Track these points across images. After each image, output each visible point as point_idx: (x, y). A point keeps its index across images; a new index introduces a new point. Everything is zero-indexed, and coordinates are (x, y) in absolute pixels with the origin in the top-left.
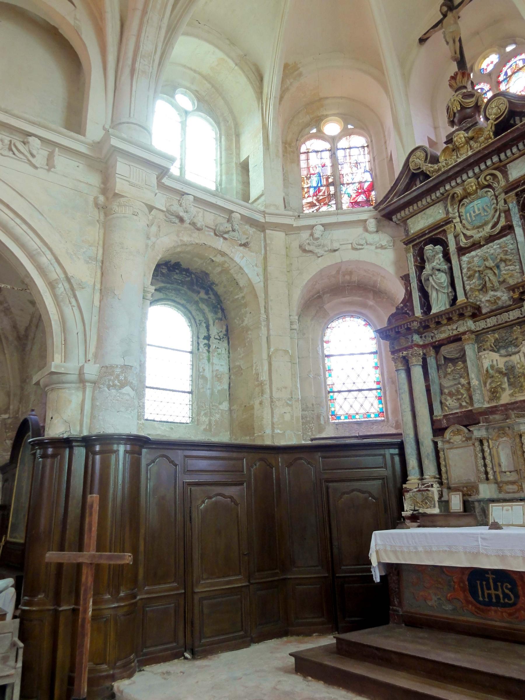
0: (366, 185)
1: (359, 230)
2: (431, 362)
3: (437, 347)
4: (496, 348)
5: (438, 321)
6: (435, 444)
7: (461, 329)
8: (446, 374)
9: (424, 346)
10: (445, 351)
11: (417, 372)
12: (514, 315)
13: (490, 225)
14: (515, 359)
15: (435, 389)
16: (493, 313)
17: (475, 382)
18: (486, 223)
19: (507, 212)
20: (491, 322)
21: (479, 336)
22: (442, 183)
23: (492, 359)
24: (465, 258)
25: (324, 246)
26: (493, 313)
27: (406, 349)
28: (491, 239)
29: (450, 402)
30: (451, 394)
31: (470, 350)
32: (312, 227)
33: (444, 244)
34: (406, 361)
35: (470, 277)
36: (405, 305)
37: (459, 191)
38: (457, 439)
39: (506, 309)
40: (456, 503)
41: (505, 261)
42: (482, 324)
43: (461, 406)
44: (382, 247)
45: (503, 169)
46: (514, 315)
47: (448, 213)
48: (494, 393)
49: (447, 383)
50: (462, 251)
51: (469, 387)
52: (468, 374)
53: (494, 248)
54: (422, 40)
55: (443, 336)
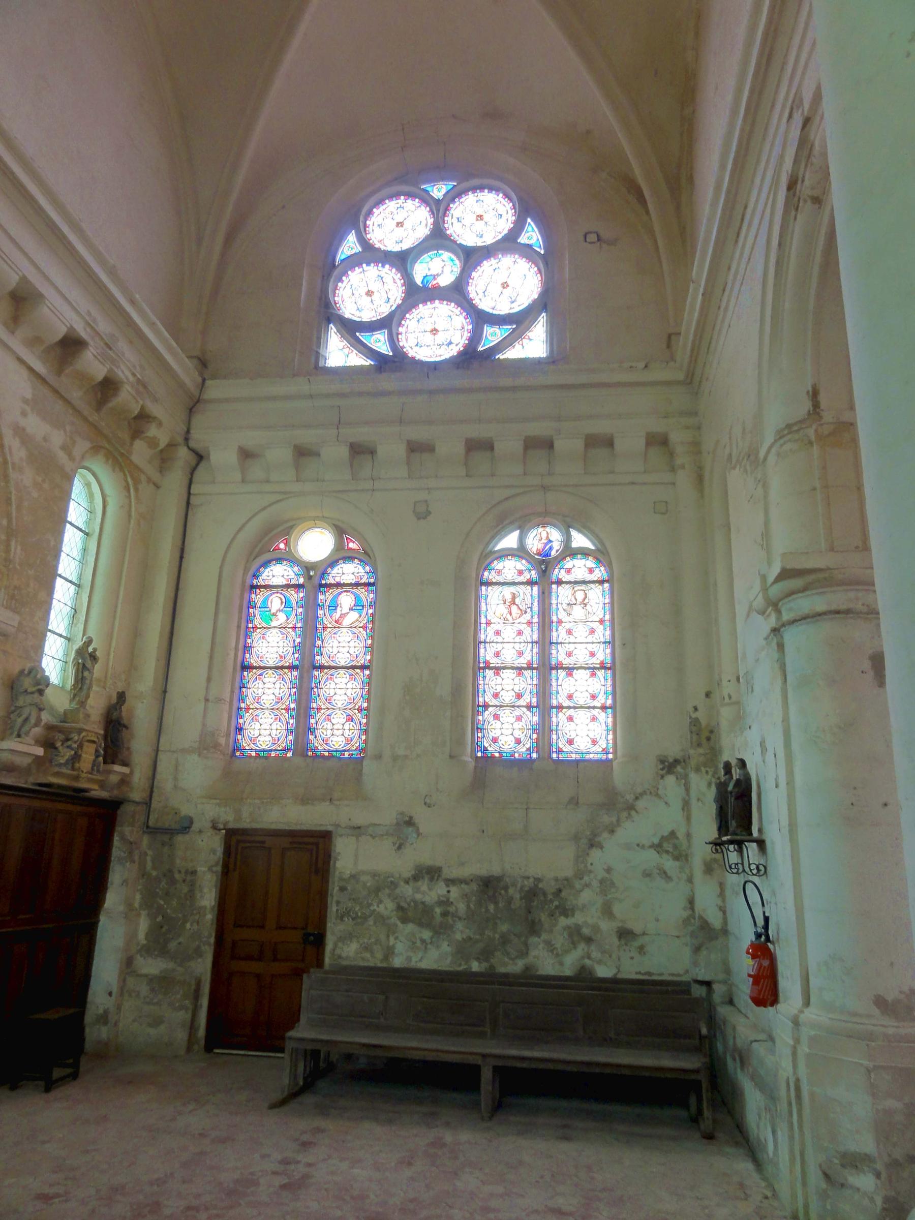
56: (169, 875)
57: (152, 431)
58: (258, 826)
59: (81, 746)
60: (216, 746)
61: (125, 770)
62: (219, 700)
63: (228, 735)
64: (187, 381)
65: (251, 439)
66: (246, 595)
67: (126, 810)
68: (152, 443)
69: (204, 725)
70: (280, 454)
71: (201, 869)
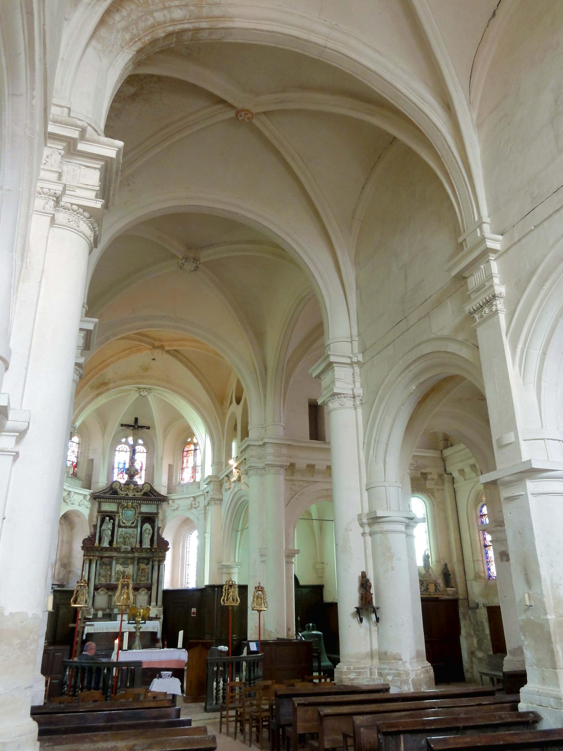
0: (75, 464)
1: (82, 497)
2: (98, 562)
3: (102, 558)
4: (121, 564)
5: (106, 549)
6: (94, 593)
7: (114, 555)
8: (101, 568)
9: (98, 556)
10: (104, 560)
11: (94, 565)
12: (130, 555)
13: (131, 522)
14: (126, 570)
15: (97, 573)
16: (124, 552)
17: (113, 574)
18: (130, 520)
19: (138, 520)
20: (123, 555)
21: (117, 559)
22: (121, 499)
23: (120, 568)
24: (120, 529)
25: (71, 501)
26: (124, 552)
27: (93, 556)
28: (130, 527)
29: (103, 579)
30: (103, 576)
31: (114, 563)
32: (70, 492)
33: (114, 521)
34: (90, 561)
35: (120, 538)
36: (92, 537)
37: (126, 504)
38: (102, 592)
39: (128, 552)
40: (100, 614)
41: (133, 537)
42: (120, 555)
43: (106, 581)
44: (87, 508)
45: (140, 505)
46: (130, 555)
47: (118, 509)
48: (118, 579)
49: (103, 572)
50: (120, 526)
51: (111, 575)
52: (111, 572)
53: (130, 531)
54: (122, 425)
55: (107, 555)
56: (477, 623)
57: (429, 477)
58: (493, 605)
59: (428, 585)
60: (480, 577)
61: (454, 589)
62: (478, 560)
63: (484, 572)
64: (435, 455)
65: (460, 466)
66: (479, 520)
67: (460, 602)
68: (433, 479)
69: (475, 570)
70: (467, 470)
71: (484, 621)
